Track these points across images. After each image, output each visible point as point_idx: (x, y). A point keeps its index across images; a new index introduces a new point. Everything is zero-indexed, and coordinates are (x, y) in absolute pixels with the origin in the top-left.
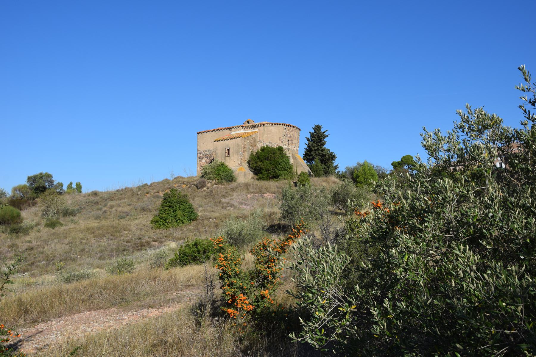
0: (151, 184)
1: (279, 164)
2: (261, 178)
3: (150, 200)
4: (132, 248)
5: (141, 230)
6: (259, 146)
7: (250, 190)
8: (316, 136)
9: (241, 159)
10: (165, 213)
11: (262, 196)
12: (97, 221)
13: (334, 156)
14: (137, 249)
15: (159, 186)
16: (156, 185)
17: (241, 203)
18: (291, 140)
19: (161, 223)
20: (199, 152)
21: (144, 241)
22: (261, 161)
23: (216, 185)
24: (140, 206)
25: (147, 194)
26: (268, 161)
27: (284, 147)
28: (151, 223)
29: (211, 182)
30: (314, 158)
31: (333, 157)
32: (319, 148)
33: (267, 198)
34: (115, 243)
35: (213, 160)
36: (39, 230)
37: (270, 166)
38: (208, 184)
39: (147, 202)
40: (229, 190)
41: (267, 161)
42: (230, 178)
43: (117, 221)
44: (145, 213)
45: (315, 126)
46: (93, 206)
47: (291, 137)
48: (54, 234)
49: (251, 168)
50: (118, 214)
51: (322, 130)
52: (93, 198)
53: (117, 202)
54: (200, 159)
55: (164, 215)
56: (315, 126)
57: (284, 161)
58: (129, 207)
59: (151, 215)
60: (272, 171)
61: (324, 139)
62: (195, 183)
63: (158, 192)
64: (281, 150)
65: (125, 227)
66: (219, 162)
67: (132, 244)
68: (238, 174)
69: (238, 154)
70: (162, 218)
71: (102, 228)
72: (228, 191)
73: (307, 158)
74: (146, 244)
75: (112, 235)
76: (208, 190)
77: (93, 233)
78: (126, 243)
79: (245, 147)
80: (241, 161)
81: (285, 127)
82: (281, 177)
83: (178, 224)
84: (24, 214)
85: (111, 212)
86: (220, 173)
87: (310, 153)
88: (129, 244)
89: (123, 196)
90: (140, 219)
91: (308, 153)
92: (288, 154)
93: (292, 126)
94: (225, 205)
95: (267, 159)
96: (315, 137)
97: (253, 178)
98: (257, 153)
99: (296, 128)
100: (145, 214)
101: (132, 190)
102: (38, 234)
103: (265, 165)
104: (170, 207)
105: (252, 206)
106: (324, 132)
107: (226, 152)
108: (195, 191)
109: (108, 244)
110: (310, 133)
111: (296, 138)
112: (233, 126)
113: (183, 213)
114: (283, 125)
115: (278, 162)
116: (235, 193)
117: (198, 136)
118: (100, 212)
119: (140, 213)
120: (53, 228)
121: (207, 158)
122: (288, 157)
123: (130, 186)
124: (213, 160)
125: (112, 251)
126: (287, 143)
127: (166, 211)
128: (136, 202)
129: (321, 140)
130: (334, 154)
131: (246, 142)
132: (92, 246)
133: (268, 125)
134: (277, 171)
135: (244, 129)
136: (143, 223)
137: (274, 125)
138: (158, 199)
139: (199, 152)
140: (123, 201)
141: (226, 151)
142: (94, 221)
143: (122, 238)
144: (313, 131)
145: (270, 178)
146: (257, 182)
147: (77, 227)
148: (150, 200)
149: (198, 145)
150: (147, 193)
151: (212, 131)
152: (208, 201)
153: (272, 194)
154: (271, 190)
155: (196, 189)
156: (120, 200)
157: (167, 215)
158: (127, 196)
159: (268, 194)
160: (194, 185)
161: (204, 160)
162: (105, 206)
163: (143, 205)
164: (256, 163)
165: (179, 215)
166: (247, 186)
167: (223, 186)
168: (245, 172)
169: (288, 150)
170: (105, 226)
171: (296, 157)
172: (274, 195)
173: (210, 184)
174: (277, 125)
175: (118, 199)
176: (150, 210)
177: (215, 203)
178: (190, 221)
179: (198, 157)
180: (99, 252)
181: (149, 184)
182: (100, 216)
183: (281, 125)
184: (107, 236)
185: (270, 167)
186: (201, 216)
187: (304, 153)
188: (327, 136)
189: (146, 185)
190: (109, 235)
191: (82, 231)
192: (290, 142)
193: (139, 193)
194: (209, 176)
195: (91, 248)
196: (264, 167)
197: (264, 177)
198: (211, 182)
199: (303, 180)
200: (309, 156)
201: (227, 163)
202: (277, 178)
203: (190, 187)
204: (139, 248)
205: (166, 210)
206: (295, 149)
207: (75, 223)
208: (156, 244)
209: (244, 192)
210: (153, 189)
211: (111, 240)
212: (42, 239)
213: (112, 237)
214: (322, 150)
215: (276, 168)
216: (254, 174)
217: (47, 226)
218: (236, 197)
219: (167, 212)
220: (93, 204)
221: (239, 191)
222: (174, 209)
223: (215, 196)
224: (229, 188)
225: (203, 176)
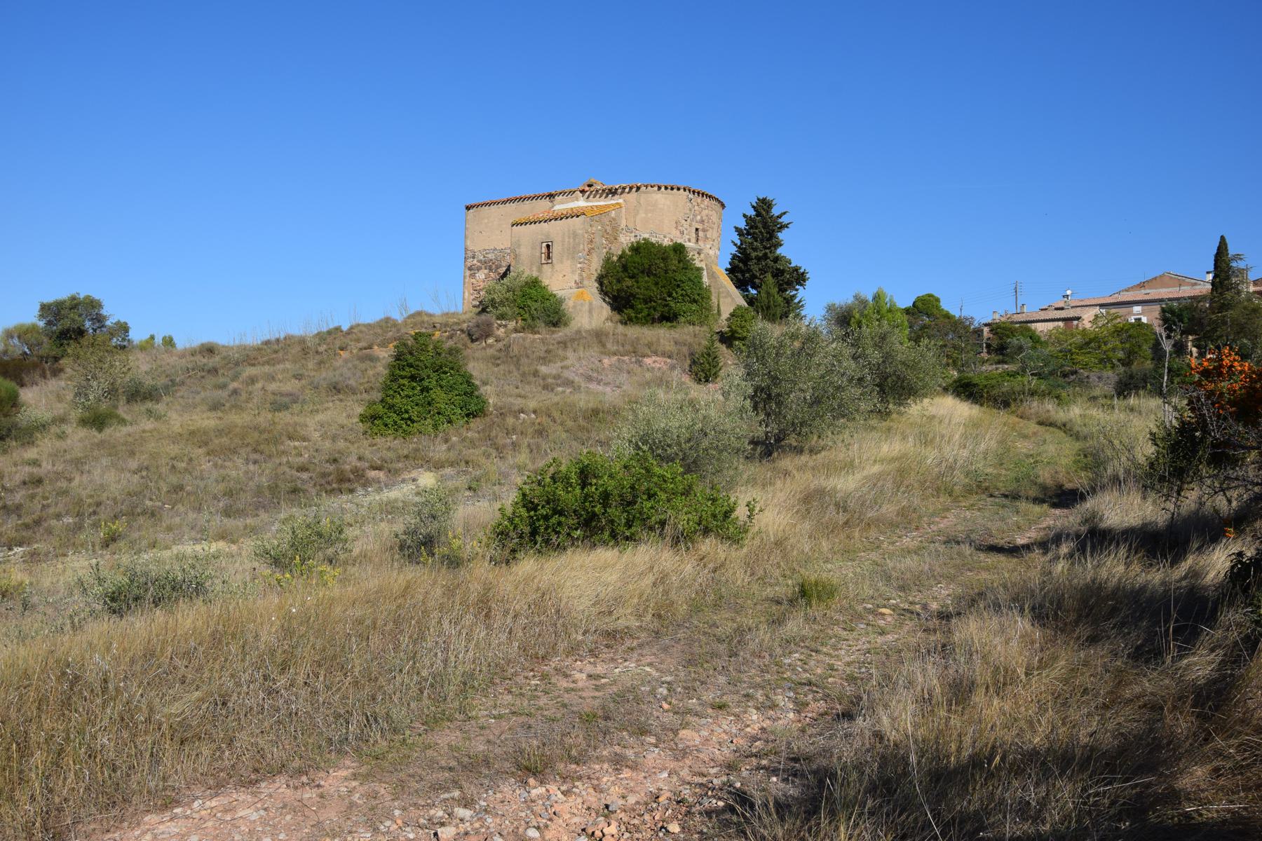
0: (352, 328)
1: (678, 286)
2: (630, 319)
3: (350, 365)
4: (315, 485)
5: (334, 438)
6: (626, 240)
7: (609, 346)
8: (760, 225)
9: (582, 270)
10: (399, 394)
11: (639, 363)
12: (213, 414)
13: (803, 273)
14: (329, 488)
15: (371, 332)
16: (364, 329)
17: (589, 379)
18: (704, 230)
19: (389, 421)
20: (468, 254)
21: (348, 467)
22: (630, 277)
23: (520, 332)
24: (325, 379)
25: (342, 352)
26: (648, 276)
27: (687, 244)
28: (362, 421)
29: (505, 326)
30: (754, 277)
31: (799, 278)
32: (769, 255)
33: (653, 368)
34: (267, 471)
35: (508, 269)
36: (64, 432)
37: (655, 289)
38: (498, 329)
39: (345, 370)
40: (553, 344)
41: (647, 278)
42: (554, 316)
43: (270, 416)
44: (341, 396)
45: (758, 199)
46: (203, 377)
47: (702, 221)
48: (101, 444)
49: (606, 294)
50: (271, 398)
51: (775, 211)
52: (205, 361)
53: (267, 369)
54: (473, 272)
55: (398, 400)
56: (758, 199)
57: (689, 279)
58: (297, 382)
59: (357, 401)
60: (660, 301)
61: (779, 234)
62: (465, 326)
63: (370, 347)
64: (681, 253)
65: (290, 429)
66: (525, 275)
67: (314, 475)
68: (574, 307)
69: (573, 258)
70: (391, 407)
71: (229, 432)
72: (551, 347)
73: (736, 276)
74: (352, 476)
75: (255, 450)
76: (500, 345)
77: (206, 444)
78: (298, 471)
79: (591, 241)
80: (581, 275)
81: (691, 196)
82: (682, 319)
83: (435, 427)
84: (28, 395)
85: (251, 393)
86: (529, 302)
87: (745, 264)
88: (305, 476)
89: (280, 355)
90: (329, 413)
91: (741, 265)
92: (698, 264)
93: (706, 195)
94: (550, 380)
95: (649, 273)
96: (756, 228)
97: (610, 319)
98: (621, 257)
99: (717, 200)
100: (341, 400)
101: (302, 341)
102: (60, 444)
103: (642, 286)
104: (413, 378)
105: (618, 387)
106: (779, 217)
107: (543, 251)
108: (465, 345)
109: (246, 472)
110: (745, 216)
111: (716, 226)
112: (559, 191)
113: (450, 396)
114: (685, 190)
115: (675, 280)
116: (570, 354)
117: (466, 216)
118: (223, 394)
119: (327, 396)
120: (100, 430)
121: (491, 270)
122: (699, 270)
123: (297, 330)
124: (508, 269)
125: (259, 492)
126: (694, 235)
127: (402, 390)
128: (316, 371)
129: (771, 235)
130: (802, 271)
131: (594, 228)
132: (202, 479)
133: (649, 188)
134: (672, 304)
135: (588, 198)
136: (340, 422)
137: (663, 189)
138: (372, 364)
139: (468, 254)
140: (281, 366)
141: (544, 250)
142: (209, 414)
143: (284, 460)
144: (752, 213)
145: (653, 321)
146: (621, 328)
147: (163, 428)
148: (350, 365)
149: (465, 237)
150: (342, 349)
151: (504, 202)
152: (504, 370)
153: (665, 359)
154: (660, 349)
155: (469, 342)
156: (274, 365)
157: (405, 401)
158: (290, 356)
159: (654, 358)
160: (462, 331)
161: (481, 275)
162: (235, 378)
163: (335, 376)
164: (619, 281)
165: (438, 400)
166: (599, 336)
167: (537, 336)
168: (591, 304)
169: (699, 253)
170: (236, 426)
171: (714, 273)
172: (669, 361)
173: (502, 330)
174: (672, 189)
175: (268, 363)
176: (354, 391)
177: (524, 375)
178: (466, 419)
180: (225, 495)
181: (345, 328)
182: (222, 401)
183: (682, 190)
184: (243, 451)
185: (655, 292)
186: (495, 406)
187: (729, 267)
188: (786, 226)
189: (338, 329)
190: (249, 449)
191: (176, 438)
192: (701, 234)
193: (321, 349)
194: (502, 310)
195: (202, 484)
196: (641, 293)
197: (640, 316)
198: (505, 326)
199: (742, 327)
200: (743, 272)
201: (543, 280)
202: (671, 322)
203: (451, 337)
204: (334, 485)
205: (404, 385)
206: (711, 252)
207: (158, 418)
208: (381, 475)
209: (594, 352)
210: (358, 340)
211: (255, 462)
212: (68, 457)
213: (256, 456)
214: (777, 259)
216: (613, 309)
217: (83, 422)
218: (575, 363)
219: (406, 393)
220: (203, 374)
221: (582, 348)
222: (426, 383)
223: (518, 360)
224: (555, 342)
225: (484, 310)
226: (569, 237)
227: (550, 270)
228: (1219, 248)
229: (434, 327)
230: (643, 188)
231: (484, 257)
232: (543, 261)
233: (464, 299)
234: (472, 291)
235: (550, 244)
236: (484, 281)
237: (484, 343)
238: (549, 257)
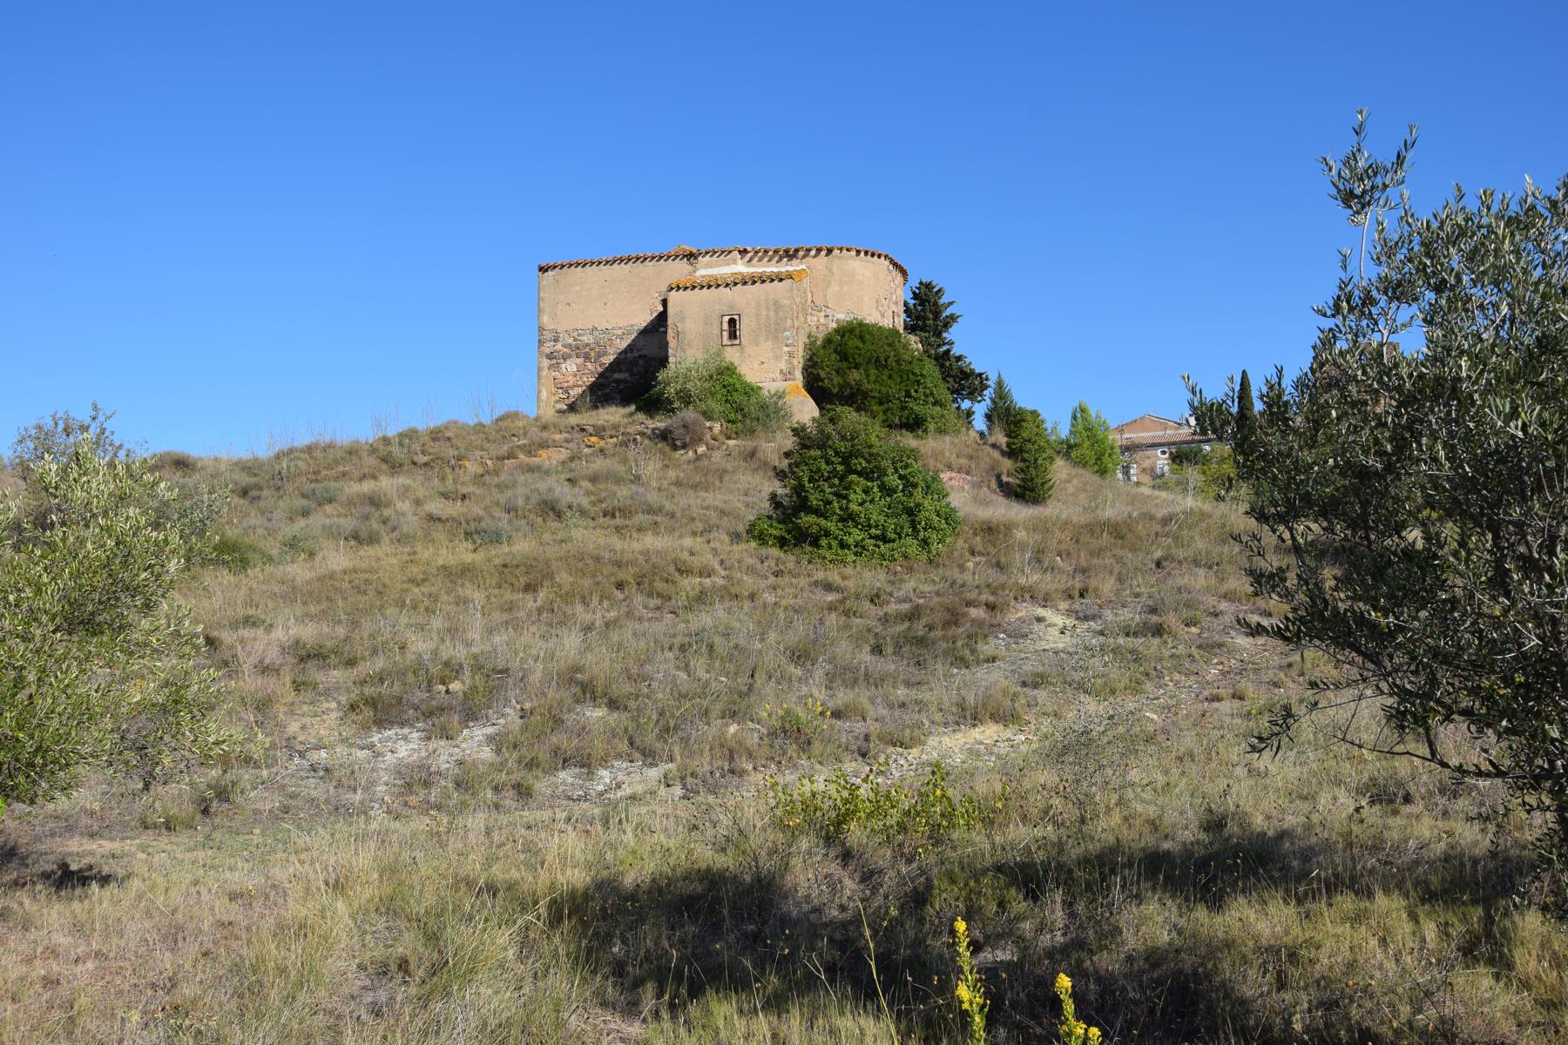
54: (554, 361)
56: (921, 283)
69: (776, 338)
115: (913, 374)
121: (587, 357)
135: (750, 261)
137: (862, 254)
141: (726, 326)
149: (539, 310)
159: (949, 474)
161: (570, 366)
174: (873, 255)
179: (540, 353)
185: (894, 389)
215: (908, 395)
226: (768, 309)
229: (583, 430)
230: (836, 252)
231: (575, 340)
232: (726, 341)
233: (539, 400)
234: (554, 390)
235: (736, 317)
236: (575, 375)
238: (733, 335)
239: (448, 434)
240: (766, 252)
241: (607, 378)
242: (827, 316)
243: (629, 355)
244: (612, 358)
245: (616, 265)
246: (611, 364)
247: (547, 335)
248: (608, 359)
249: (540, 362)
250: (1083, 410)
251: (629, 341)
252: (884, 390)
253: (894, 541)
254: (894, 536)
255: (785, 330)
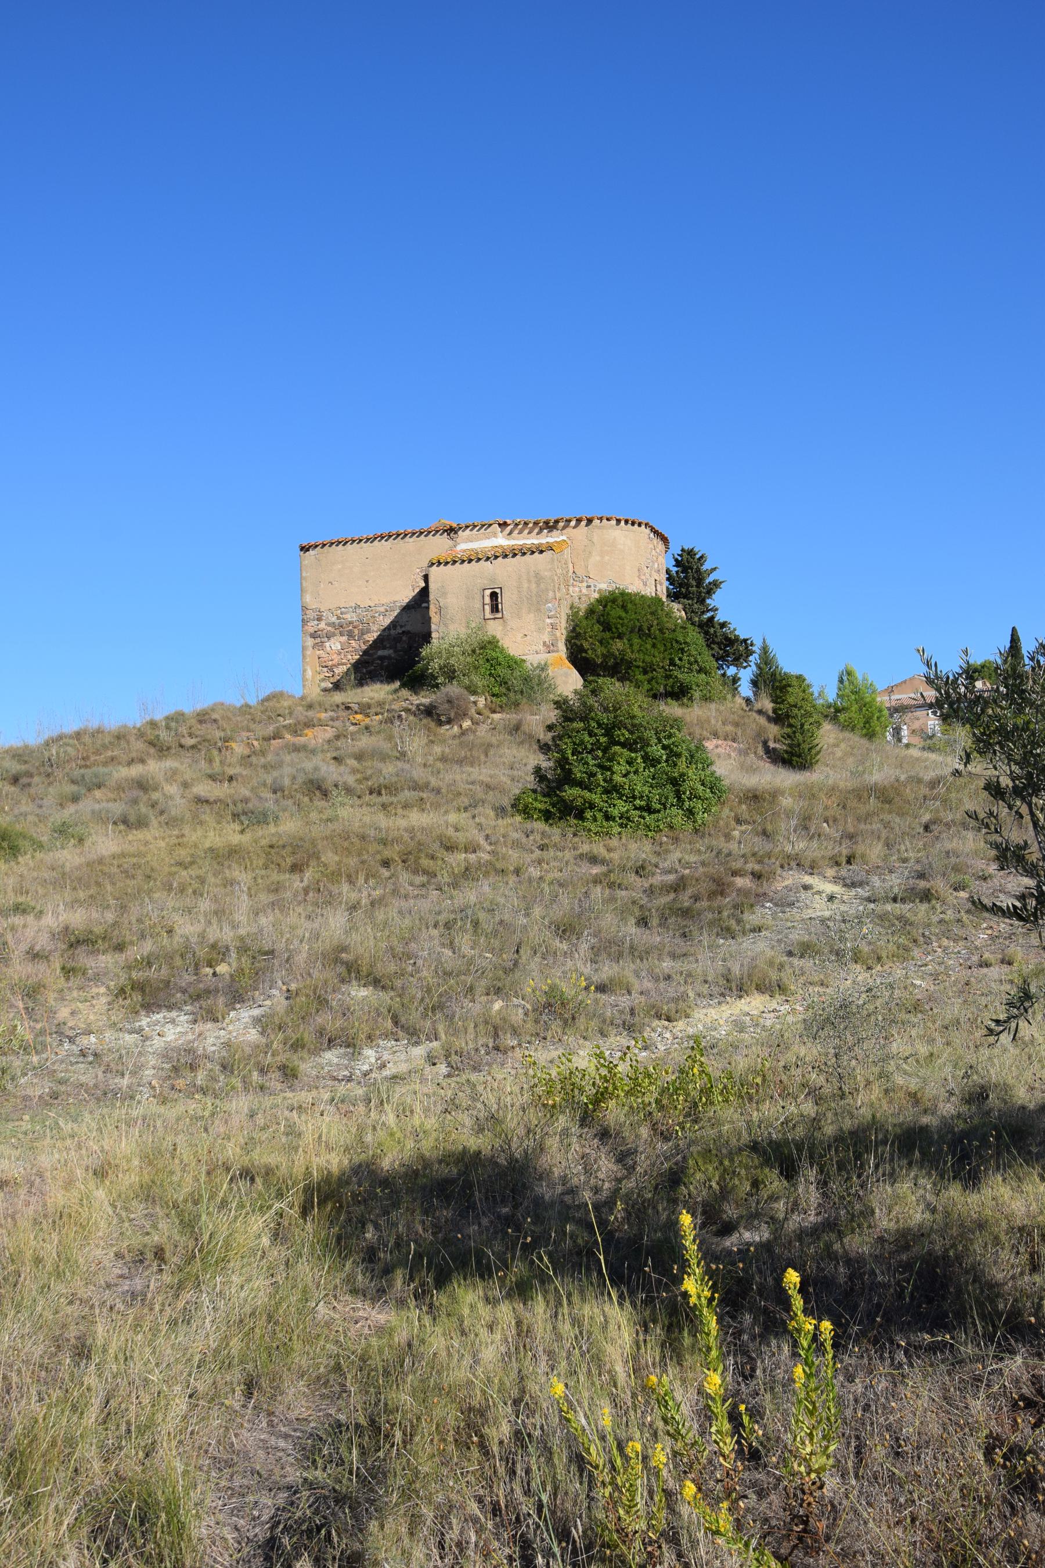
54: (318, 640)
56: (683, 550)
69: (539, 610)
81: (652, 535)
115: (677, 642)
121: (350, 635)
133: (604, 521)
135: (510, 534)
137: (623, 523)
141: (487, 600)
159: (715, 741)
161: (334, 645)
172: (735, 745)
174: (633, 524)
179: (304, 632)
183: (643, 526)
185: (658, 658)
215: (672, 663)
226: (529, 581)
227: (500, 628)
228: (1012, 635)
229: (348, 708)
230: (596, 522)
231: (338, 618)
232: (488, 615)
233: (304, 679)
235: (498, 591)
236: (339, 654)
237: (456, 728)
238: (495, 609)
239: (215, 716)
240: (526, 524)
241: (371, 655)
242: (589, 587)
243: (393, 632)
244: (375, 635)
245: (376, 542)
246: (375, 641)
247: (311, 614)
248: (371, 637)
249: (304, 642)
250: (849, 673)
251: (392, 618)
252: (648, 659)
253: (659, 811)
254: (658, 806)
255: (547, 601)
